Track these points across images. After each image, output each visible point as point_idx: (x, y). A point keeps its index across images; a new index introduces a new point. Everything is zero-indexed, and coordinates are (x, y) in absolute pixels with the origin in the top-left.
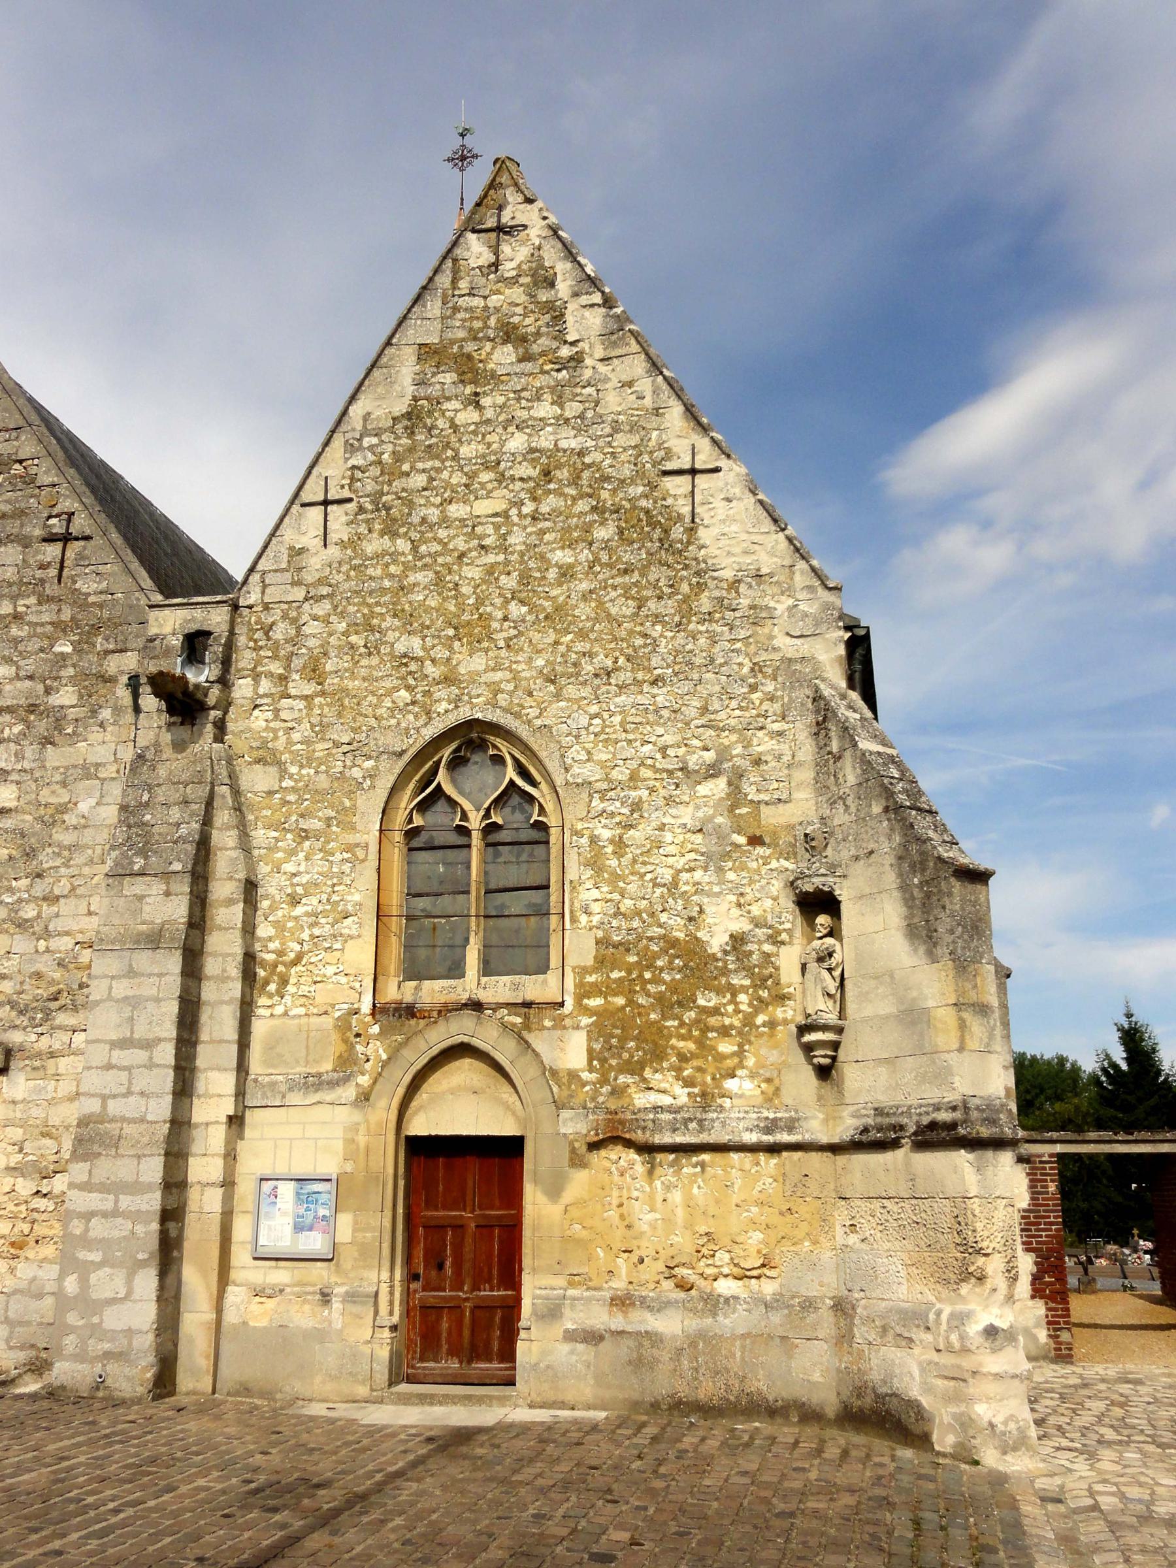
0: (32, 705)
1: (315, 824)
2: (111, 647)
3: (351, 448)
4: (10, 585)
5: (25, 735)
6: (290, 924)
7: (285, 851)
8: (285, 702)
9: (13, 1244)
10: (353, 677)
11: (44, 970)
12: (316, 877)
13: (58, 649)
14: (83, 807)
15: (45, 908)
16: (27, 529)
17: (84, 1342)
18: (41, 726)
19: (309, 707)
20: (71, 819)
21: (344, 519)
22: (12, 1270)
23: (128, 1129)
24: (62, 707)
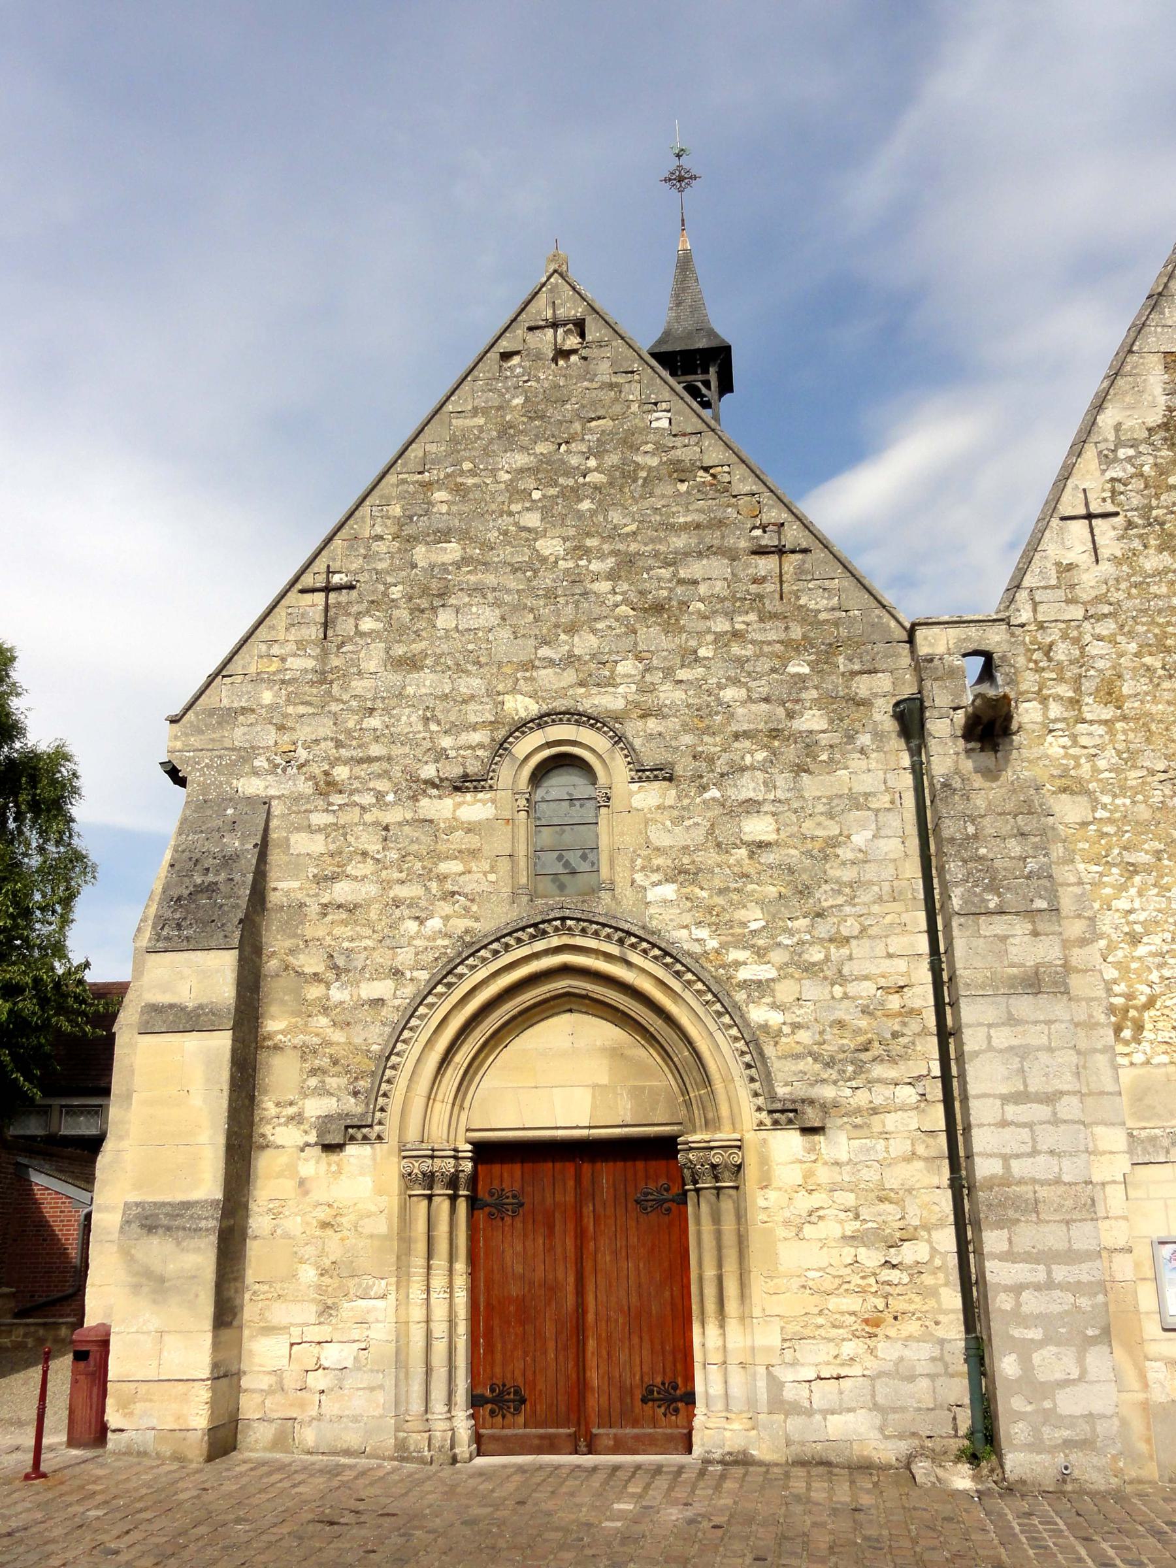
0: (774, 730)
1: (1142, 858)
2: (857, 667)
3: (1107, 459)
4: (722, 600)
6: (1134, 965)
7: (1113, 886)
8: (1081, 727)
9: (866, 1321)
10: (1155, 700)
11: (847, 1018)
12: (1154, 914)
13: (792, 669)
14: (860, 839)
15: (833, 950)
16: (731, 541)
17: (1036, 1431)
18: (791, 753)
19: (1112, 732)
20: (845, 853)
21: (1113, 534)
22: (871, 1351)
23: (1043, 1192)
24: (811, 732)
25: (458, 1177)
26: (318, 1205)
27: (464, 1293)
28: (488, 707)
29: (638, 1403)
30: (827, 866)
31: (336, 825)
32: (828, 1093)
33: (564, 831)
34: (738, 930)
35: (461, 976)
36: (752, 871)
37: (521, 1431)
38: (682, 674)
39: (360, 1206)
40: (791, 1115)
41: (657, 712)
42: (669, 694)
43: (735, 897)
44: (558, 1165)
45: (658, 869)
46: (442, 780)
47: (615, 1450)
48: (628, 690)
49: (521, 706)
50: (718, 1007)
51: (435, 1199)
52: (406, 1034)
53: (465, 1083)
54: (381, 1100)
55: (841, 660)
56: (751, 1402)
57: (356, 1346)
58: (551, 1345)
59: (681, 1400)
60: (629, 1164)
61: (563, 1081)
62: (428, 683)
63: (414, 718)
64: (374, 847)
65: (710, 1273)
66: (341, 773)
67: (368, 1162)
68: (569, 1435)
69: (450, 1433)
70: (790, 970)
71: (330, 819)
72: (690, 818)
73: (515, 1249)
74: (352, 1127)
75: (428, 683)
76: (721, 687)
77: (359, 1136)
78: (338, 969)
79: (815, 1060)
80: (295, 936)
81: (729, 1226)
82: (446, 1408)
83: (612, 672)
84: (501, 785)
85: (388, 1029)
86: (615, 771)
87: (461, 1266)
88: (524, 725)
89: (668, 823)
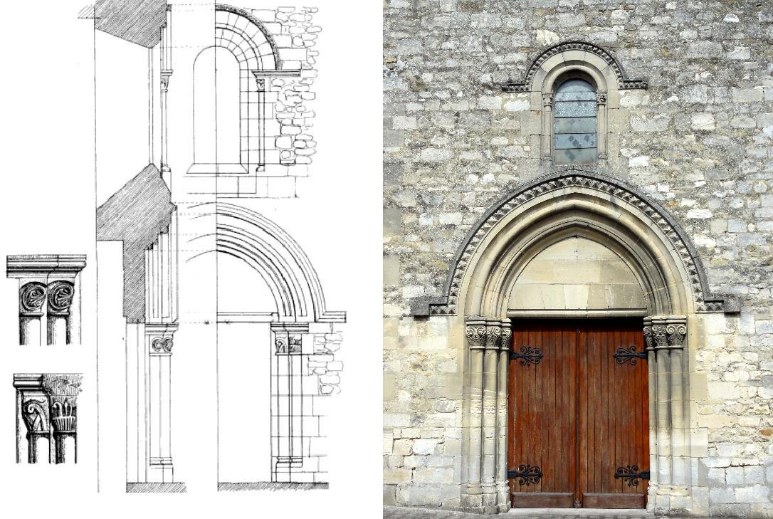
0: (716, 59)
5: (713, 79)
13: (728, 19)
15: (749, 201)
18: (725, 74)
24: (739, 61)
25: (502, 339)
26: (411, 353)
27: (505, 410)
28: (526, 37)
29: (613, 478)
30: (747, 148)
31: (424, 111)
32: (743, 291)
33: (574, 122)
34: (688, 187)
35: (506, 211)
36: (698, 149)
37: (539, 494)
38: (656, 20)
39: (439, 355)
40: (720, 304)
41: (639, 45)
42: (646, 33)
43: (686, 165)
44: (565, 333)
45: (636, 147)
46: (494, 84)
47: (598, 505)
48: (619, 29)
49: (547, 37)
50: (674, 235)
51: (487, 351)
52: (470, 247)
53: (507, 280)
54: (453, 289)
55: (760, 14)
57: (436, 441)
58: (559, 442)
59: (640, 477)
60: (610, 333)
61: (572, 281)
62: (485, 20)
63: (476, 43)
64: (449, 127)
65: (663, 400)
66: (427, 77)
67: (445, 327)
68: (569, 496)
69: (495, 495)
70: (721, 213)
71: (420, 107)
72: (658, 114)
73: (540, 386)
74: (434, 305)
75: (485, 20)
76: (681, 29)
77: (439, 311)
78: (425, 205)
79: (736, 270)
80: (396, 182)
81: (676, 372)
82: (492, 480)
83: (609, 16)
84: (533, 89)
85: (457, 245)
86: (610, 82)
87: (503, 394)
88: (550, 49)
89: (644, 117)
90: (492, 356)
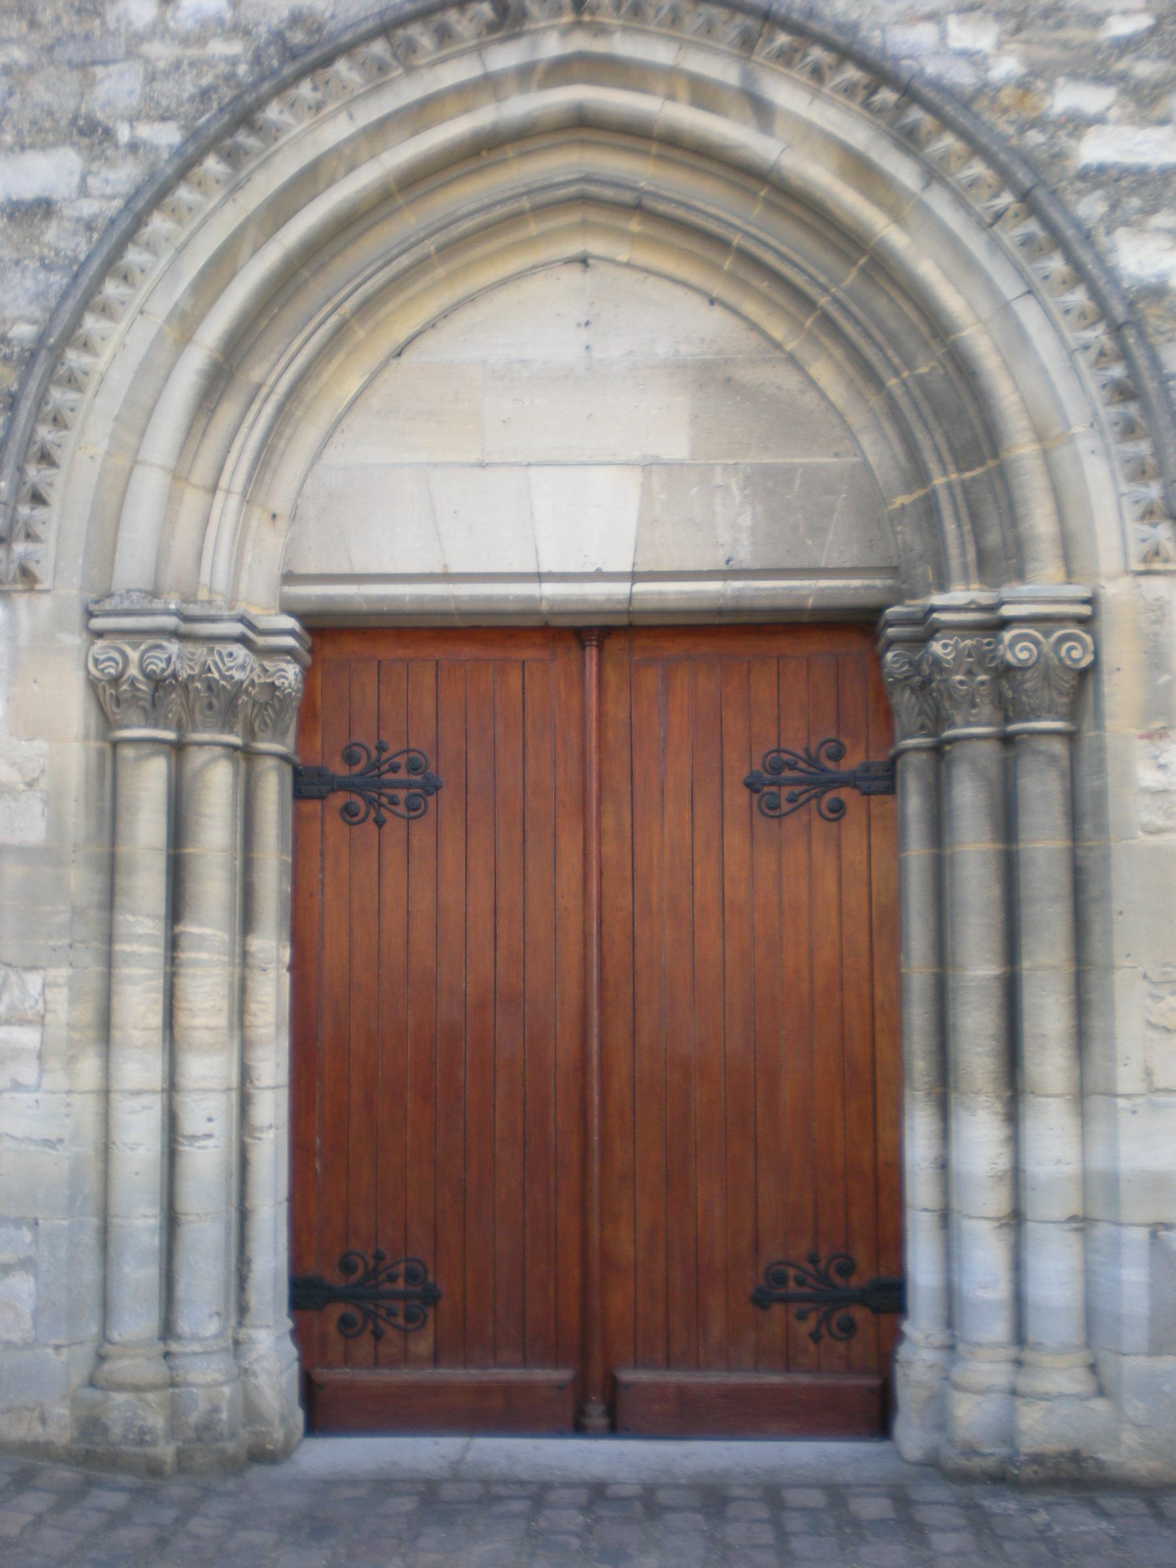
34: (1076, 34)
51: (197, 758)
56: (1093, 1318)
81: (1044, 843)
85: (58, 280)
90: (217, 781)
